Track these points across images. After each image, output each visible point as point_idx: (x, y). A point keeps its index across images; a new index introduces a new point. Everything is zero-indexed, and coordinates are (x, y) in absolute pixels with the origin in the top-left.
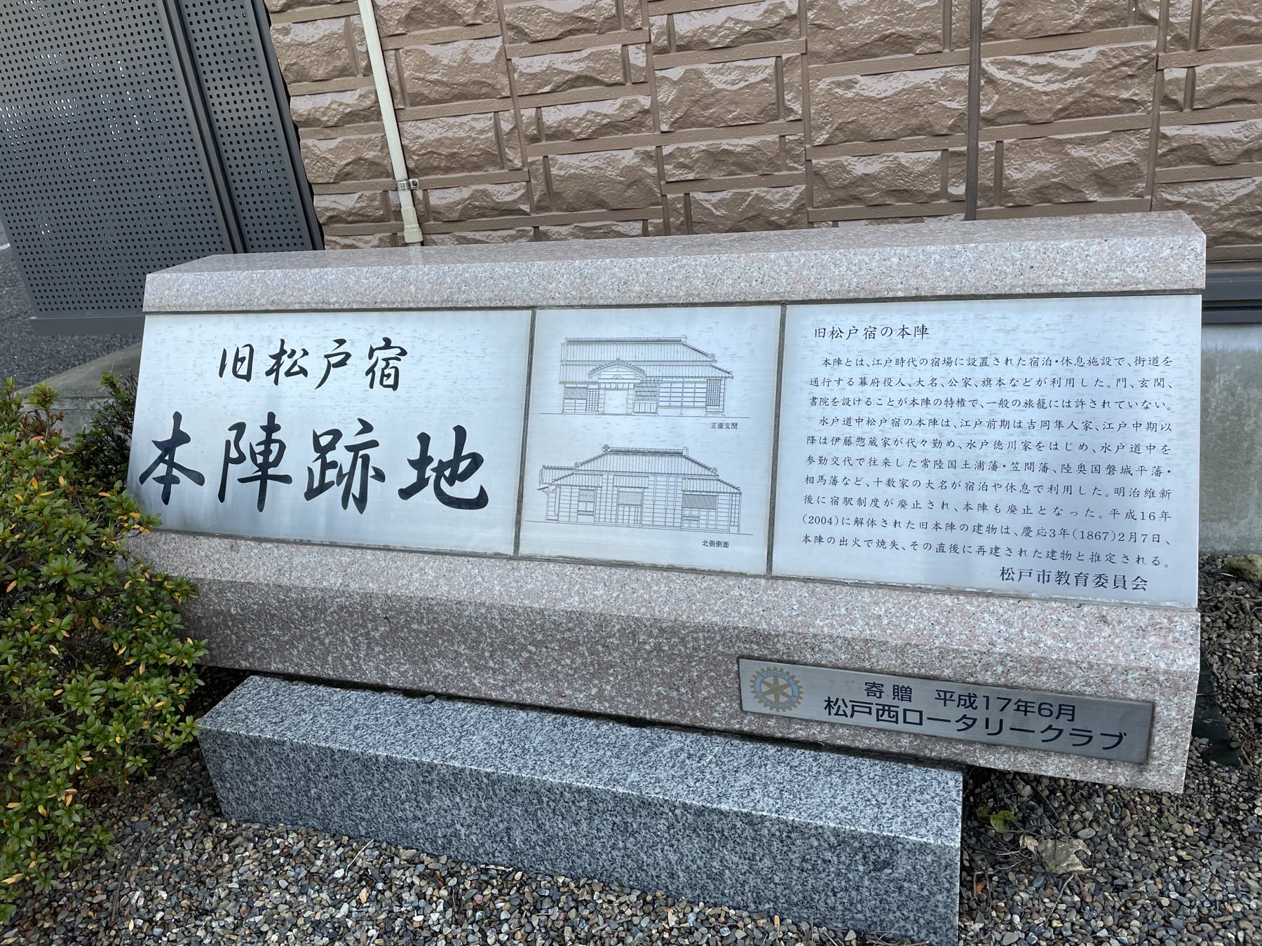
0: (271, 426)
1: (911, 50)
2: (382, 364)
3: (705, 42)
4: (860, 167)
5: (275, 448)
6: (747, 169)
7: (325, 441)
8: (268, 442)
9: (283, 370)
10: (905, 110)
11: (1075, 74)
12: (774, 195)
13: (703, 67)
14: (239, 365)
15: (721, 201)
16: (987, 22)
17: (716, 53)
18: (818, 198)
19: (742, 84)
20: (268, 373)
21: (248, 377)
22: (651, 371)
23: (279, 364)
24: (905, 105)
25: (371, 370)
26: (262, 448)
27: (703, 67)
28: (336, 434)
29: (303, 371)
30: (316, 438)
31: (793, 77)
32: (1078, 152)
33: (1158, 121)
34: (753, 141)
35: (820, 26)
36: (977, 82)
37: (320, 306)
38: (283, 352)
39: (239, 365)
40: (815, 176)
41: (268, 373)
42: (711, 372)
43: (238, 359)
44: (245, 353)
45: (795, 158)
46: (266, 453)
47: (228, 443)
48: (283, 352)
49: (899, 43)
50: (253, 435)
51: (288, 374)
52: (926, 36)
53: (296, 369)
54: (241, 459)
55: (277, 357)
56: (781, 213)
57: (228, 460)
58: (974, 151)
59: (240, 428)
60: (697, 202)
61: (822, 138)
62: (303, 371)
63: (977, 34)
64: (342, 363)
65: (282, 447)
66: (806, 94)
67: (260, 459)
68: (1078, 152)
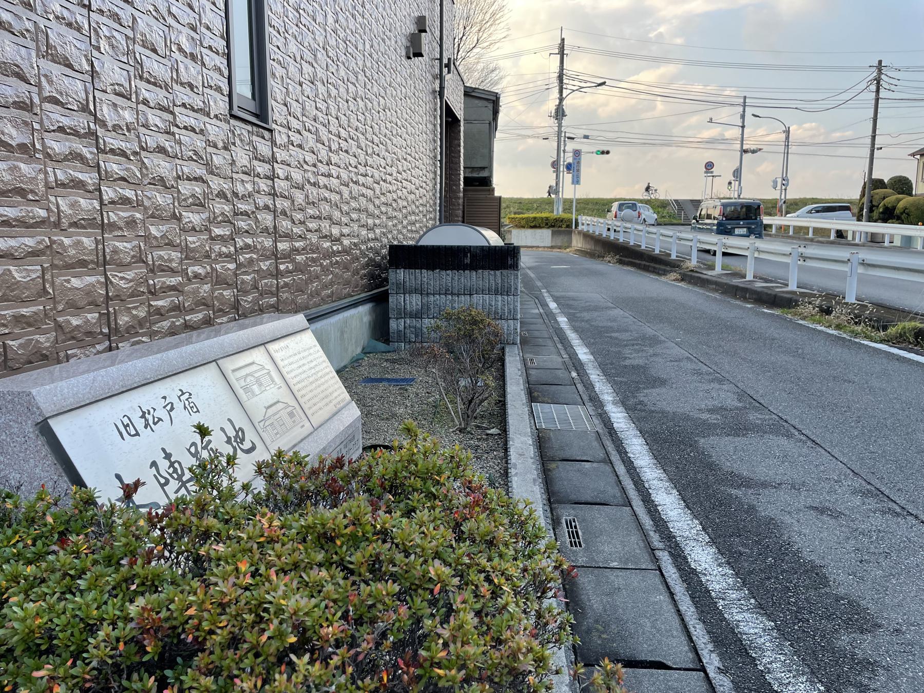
0: (168, 456)
1: (86, 267)
2: (187, 403)
3: (12, 255)
4: (75, 321)
5: (176, 465)
6: (30, 325)
7: (193, 450)
8: (172, 465)
9: (151, 422)
10: (87, 294)
11: (131, 281)
12: (42, 338)
13: (11, 268)
14: (127, 429)
15: (20, 345)
16: (108, 257)
17: (16, 261)
18: (60, 339)
19: (29, 279)
20: (146, 427)
21: (137, 434)
22: (256, 375)
23: (147, 420)
24: (88, 291)
25: (185, 408)
26: (172, 469)
27: (11, 268)
28: (194, 444)
29: (160, 419)
30: (189, 450)
31: (48, 276)
32: (134, 312)
33: (149, 300)
34: (34, 309)
35: (58, 252)
36: (107, 283)
37: (145, 382)
38: (144, 413)
39: (127, 429)
40: (59, 327)
41: (146, 427)
42: (266, 371)
43: (126, 426)
44: (126, 421)
45: (49, 318)
46: (175, 470)
47: (155, 476)
48: (144, 413)
49: (83, 263)
50: (164, 465)
51: (155, 424)
52: (92, 262)
53: (156, 420)
54: (167, 482)
55: (143, 416)
56: (46, 348)
57: (162, 486)
58: (108, 313)
59: (154, 464)
60: (10, 346)
61: (60, 308)
62: (160, 419)
63: (105, 263)
64: (172, 409)
65: (180, 463)
66: (53, 284)
67: (175, 476)
68: (134, 312)
